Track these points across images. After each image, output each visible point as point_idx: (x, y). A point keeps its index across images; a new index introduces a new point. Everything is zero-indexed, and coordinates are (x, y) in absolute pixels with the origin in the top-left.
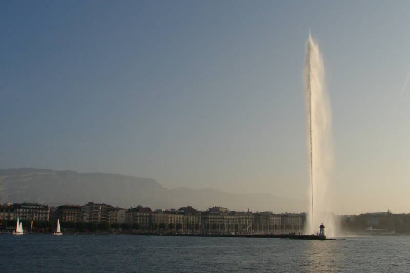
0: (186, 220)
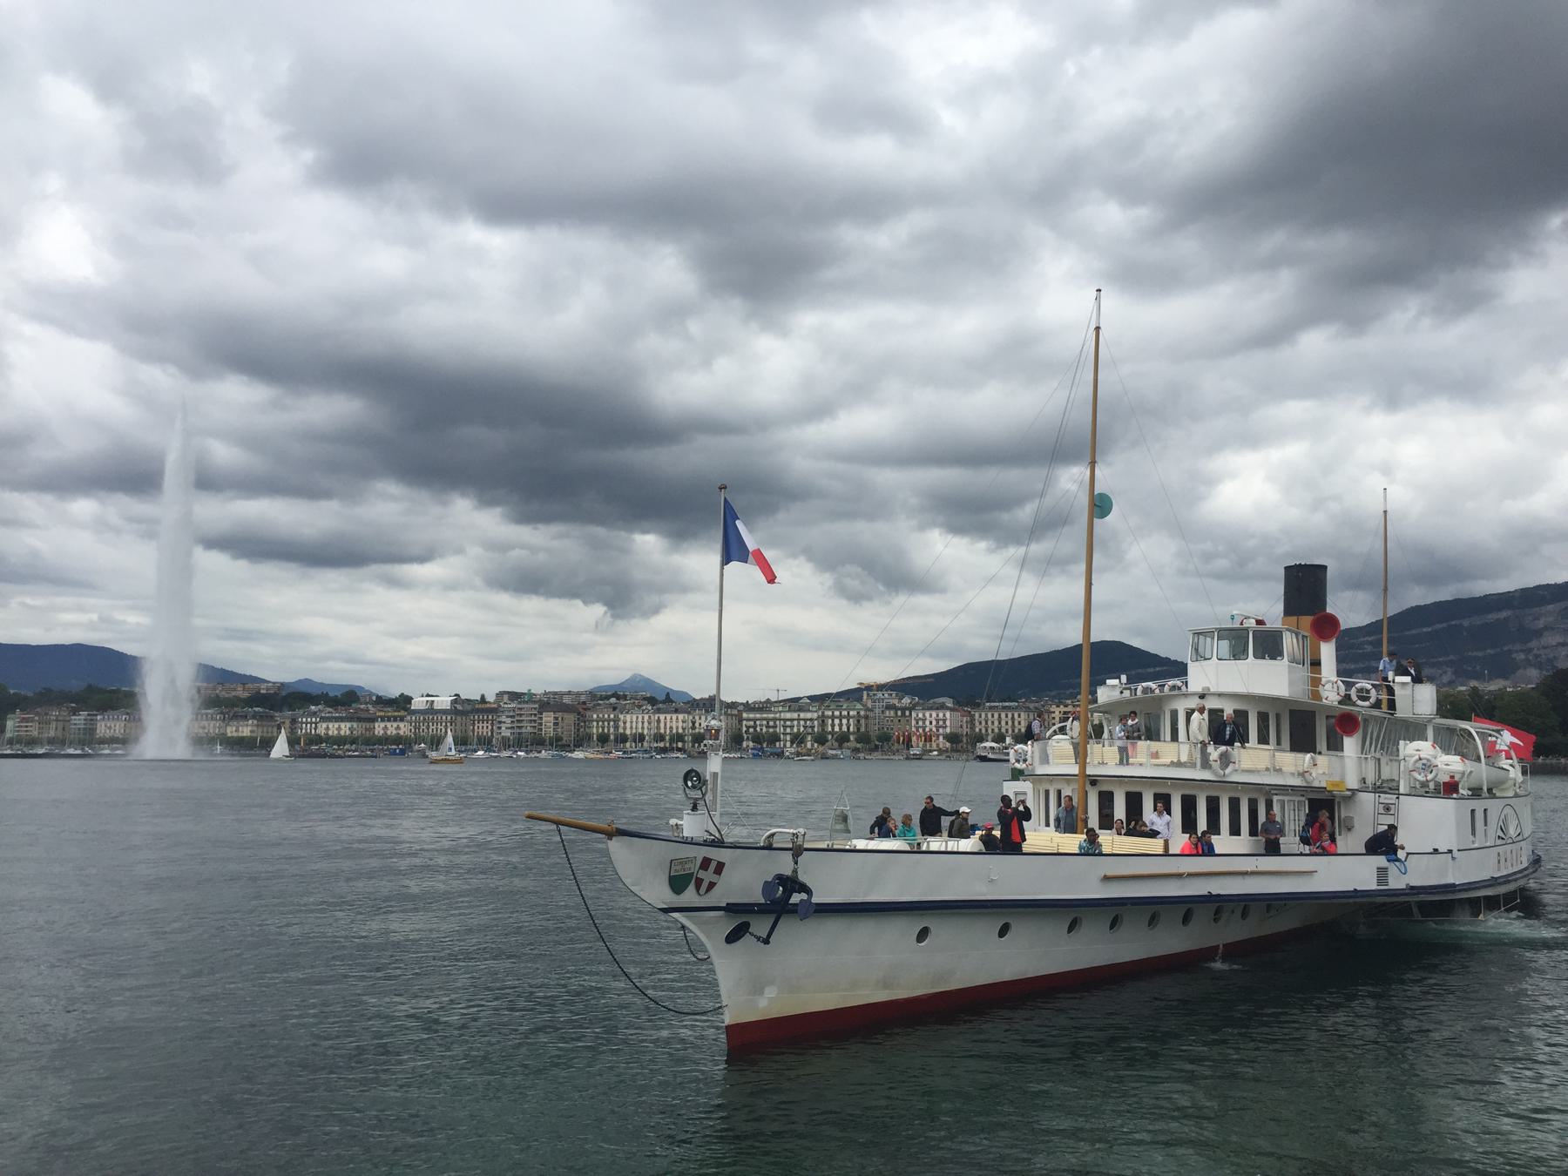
0: (691, 725)
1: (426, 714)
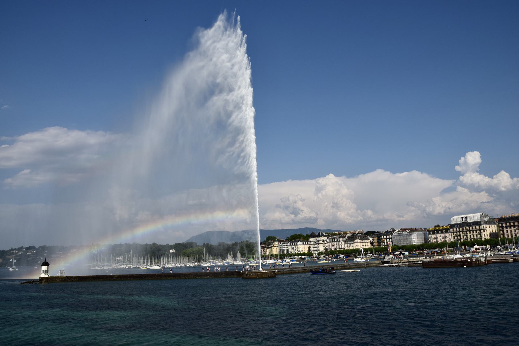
1: (464, 226)
